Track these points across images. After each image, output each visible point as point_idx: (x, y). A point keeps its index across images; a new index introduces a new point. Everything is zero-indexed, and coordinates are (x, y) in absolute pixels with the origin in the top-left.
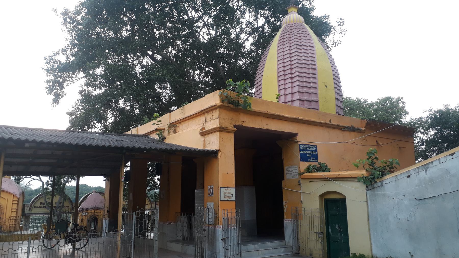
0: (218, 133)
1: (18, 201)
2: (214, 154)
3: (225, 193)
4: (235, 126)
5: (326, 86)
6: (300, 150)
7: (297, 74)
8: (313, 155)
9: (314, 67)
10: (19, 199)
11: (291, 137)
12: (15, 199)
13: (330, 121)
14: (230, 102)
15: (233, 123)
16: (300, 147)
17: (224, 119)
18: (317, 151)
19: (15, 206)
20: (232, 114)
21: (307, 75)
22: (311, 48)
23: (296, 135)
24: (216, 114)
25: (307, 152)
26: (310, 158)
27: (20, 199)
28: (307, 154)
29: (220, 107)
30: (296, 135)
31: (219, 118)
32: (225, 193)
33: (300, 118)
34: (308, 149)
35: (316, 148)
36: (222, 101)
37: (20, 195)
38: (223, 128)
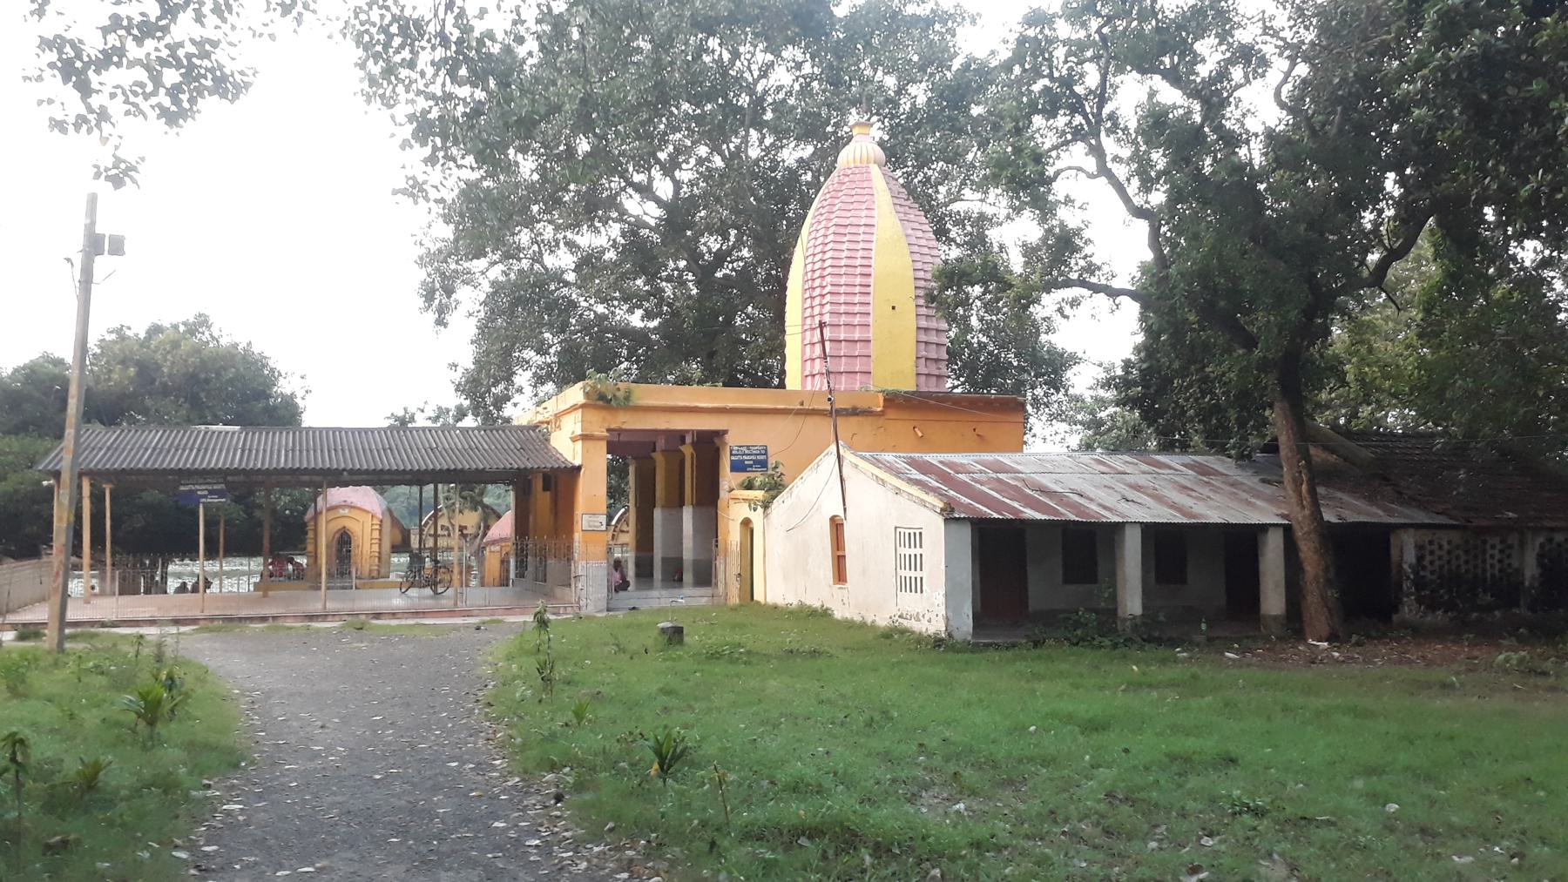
0: (580, 442)
1: (380, 526)
2: (579, 468)
3: (589, 522)
4: (608, 430)
5: (893, 308)
6: (731, 455)
7: (828, 289)
8: (756, 462)
9: (866, 270)
10: (381, 521)
11: (720, 434)
12: (376, 521)
13: (802, 404)
14: (602, 397)
15: (606, 426)
16: (731, 451)
17: (590, 422)
18: (766, 454)
19: (376, 534)
20: (604, 414)
21: (849, 290)
22: (868, 230)
23: (725, 432)
24: (578, 414)
25: (745, 457)
26: (751, 466)
27: (384, 521)
28: (744, 461)
29: (583, 406)
30: (725, 432)
31: (582, 421)
32: (589, 522)
33: (731, 405)
34: (747, 452)
35: (766, 451)
36: (587, 395)
37: (383, 514)
38: (586, 435)
